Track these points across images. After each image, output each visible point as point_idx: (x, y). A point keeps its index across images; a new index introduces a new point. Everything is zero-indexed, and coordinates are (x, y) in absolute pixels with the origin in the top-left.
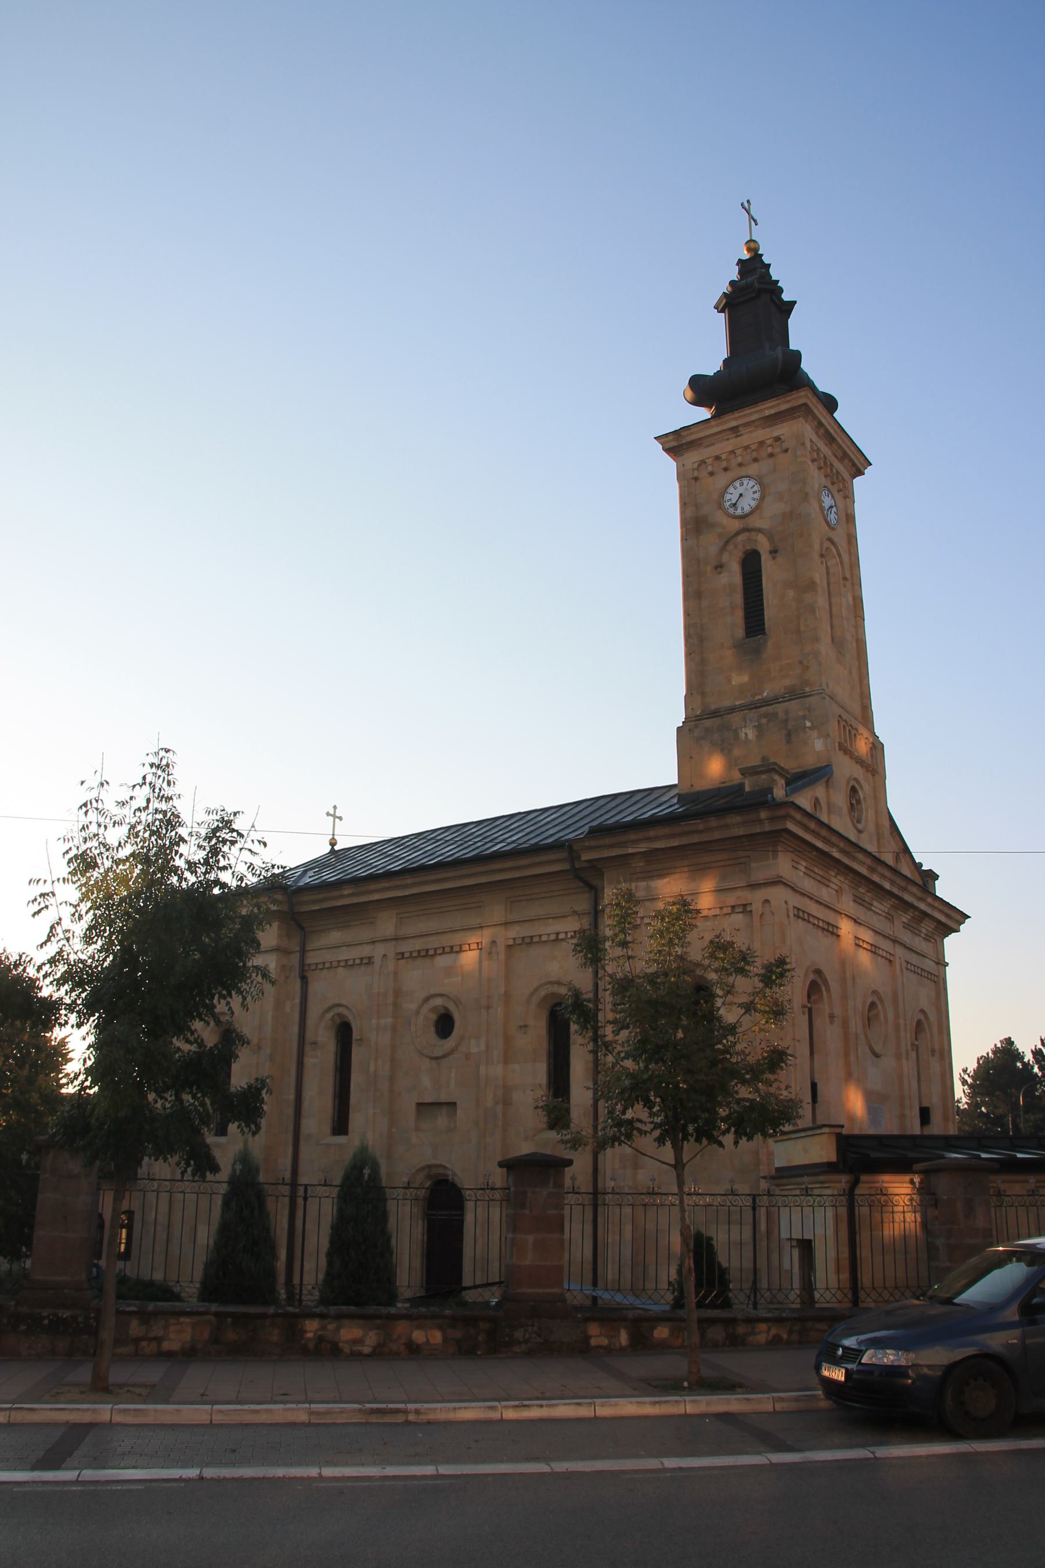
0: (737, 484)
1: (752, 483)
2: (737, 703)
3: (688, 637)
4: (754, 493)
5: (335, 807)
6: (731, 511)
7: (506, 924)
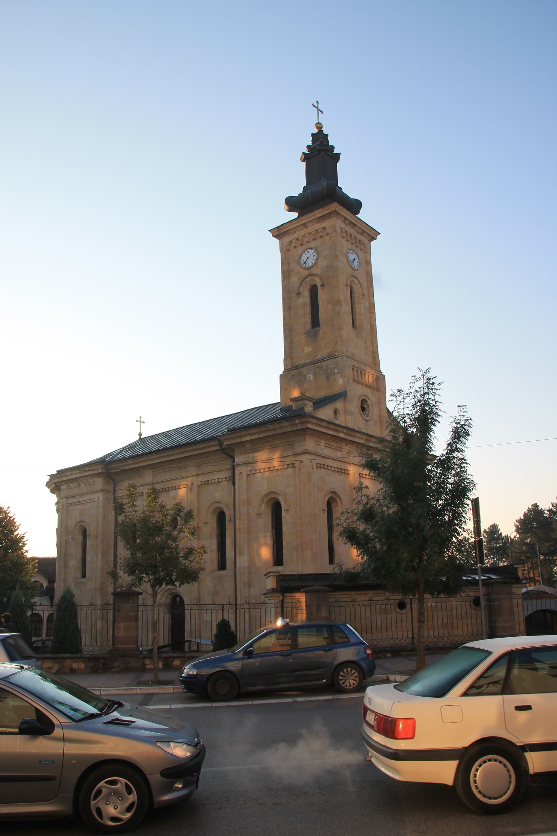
0: (306, 252)
1: (313, 251)
2: (307, 362)
4: (314, 256)
5: (140, 417)
6: (304, 266)
7: (197, 475)
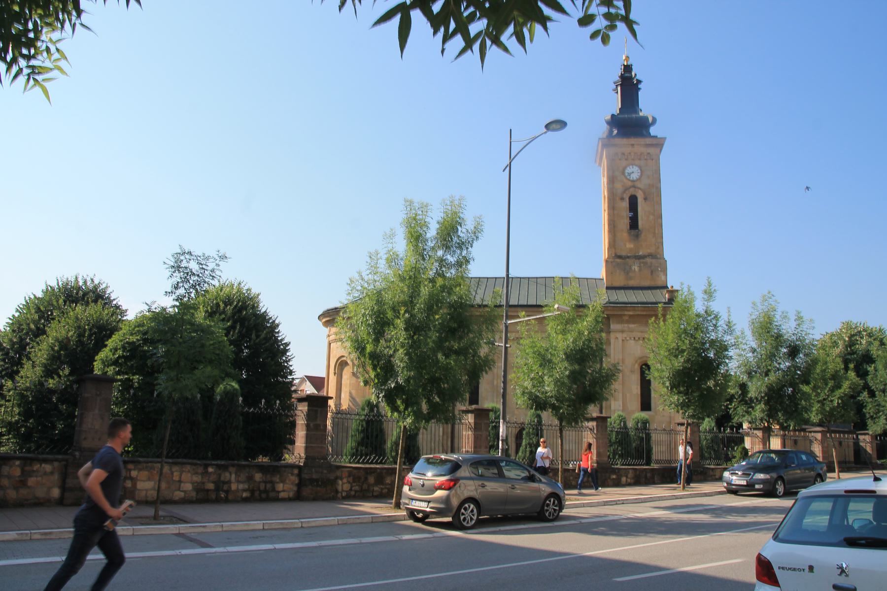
3: (609, 224)
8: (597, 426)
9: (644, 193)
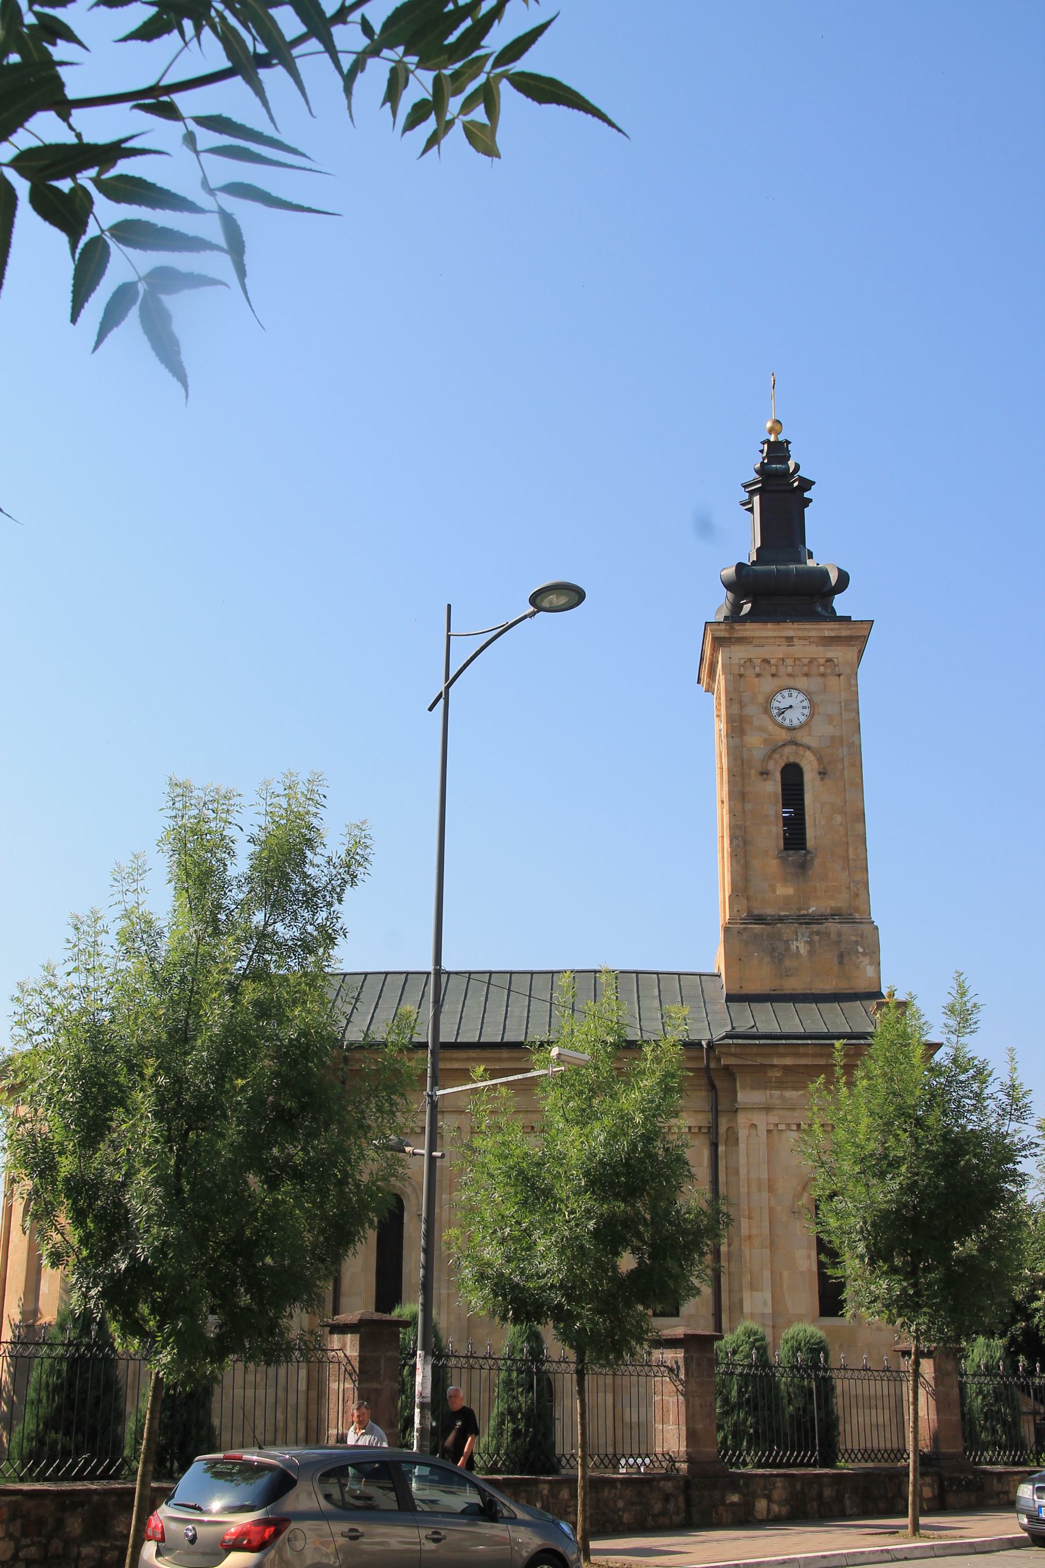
0: (786, 693)
1: (801, 697)
2: (783, 913)
3: (733, 838)
6: (779, 719)
8: (686, 1359)
9: (820, 760)
